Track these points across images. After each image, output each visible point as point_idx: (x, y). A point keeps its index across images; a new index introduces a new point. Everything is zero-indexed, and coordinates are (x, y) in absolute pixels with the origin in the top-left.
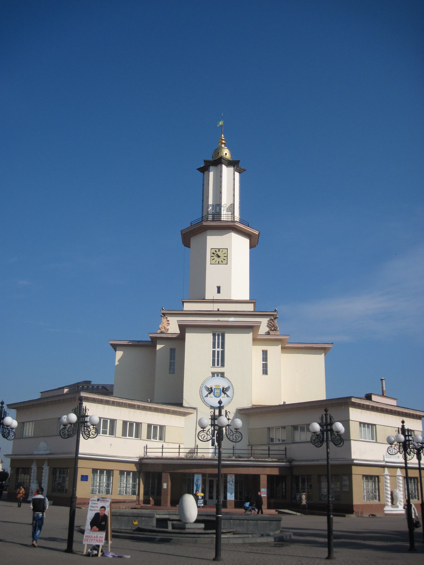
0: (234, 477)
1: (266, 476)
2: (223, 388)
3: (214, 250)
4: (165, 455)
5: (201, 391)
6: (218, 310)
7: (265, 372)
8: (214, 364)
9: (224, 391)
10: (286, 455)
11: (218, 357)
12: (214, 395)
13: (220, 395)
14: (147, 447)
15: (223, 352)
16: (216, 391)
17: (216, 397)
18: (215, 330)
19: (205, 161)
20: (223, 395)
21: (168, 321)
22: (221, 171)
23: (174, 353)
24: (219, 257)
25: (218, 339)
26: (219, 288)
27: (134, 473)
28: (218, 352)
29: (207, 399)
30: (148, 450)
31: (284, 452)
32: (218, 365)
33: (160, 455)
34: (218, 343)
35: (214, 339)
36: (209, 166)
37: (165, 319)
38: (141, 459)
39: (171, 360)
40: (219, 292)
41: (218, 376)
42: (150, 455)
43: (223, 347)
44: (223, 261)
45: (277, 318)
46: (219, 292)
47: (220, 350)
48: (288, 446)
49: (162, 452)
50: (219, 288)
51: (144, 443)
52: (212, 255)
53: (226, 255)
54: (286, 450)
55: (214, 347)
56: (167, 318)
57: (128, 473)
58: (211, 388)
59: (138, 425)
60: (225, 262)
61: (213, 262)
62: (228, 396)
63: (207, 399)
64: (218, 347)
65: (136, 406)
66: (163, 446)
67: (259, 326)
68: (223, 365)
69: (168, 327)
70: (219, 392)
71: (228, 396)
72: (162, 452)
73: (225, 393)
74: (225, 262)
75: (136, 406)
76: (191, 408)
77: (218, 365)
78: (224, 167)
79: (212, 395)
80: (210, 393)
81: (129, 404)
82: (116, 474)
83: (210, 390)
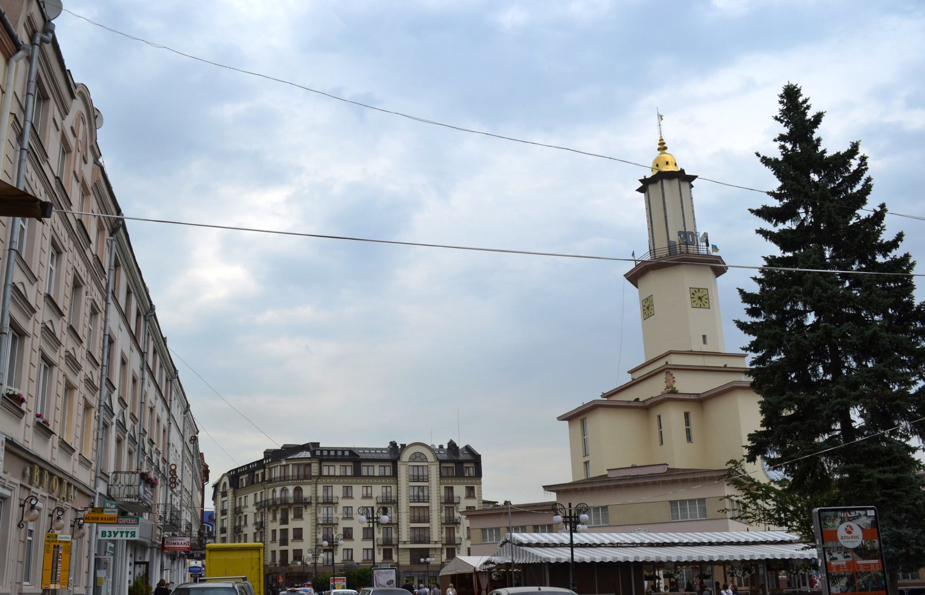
6: (725, 366)
24: (700, 298)
26: (704, 337)
40: (705, 342)
46: (705, 342)
50: (704, 337)
74: (707, 305)
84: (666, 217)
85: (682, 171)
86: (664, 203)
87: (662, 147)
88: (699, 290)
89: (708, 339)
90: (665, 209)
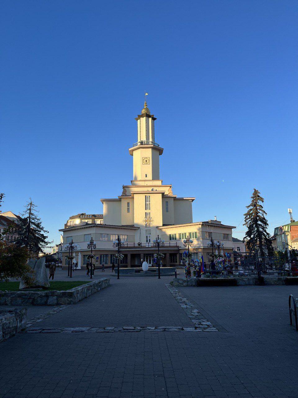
7: (167, 211)
8: (146, 209)
11: (148, 206)
15: (150, 204)
18: (146, 195)
24: (146, 161)
40: (146, 177)
43: (149, 202)
46: (146, 177)
53: (149, 160)
67: (164, 193)
68: (150, 209)
82: (109, 256)
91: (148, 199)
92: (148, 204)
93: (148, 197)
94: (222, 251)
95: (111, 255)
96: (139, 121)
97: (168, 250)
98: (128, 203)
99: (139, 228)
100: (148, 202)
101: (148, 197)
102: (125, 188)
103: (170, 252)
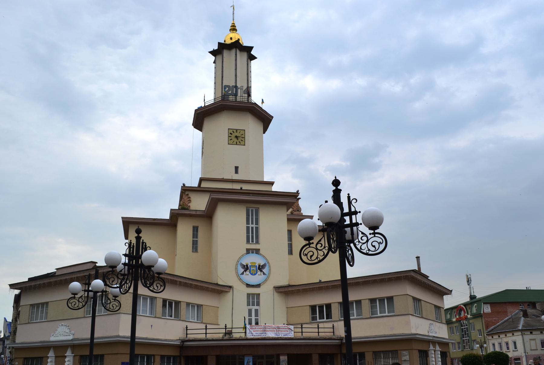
0: (286, 357)
1: (318, 355)
2: (259, 266)
3: (231, 130)
4: (209, 336)
5: (236, 269)
6: (241, 189)
8: (248, 241)
9: (261, 268)
10: (334, 332)
11: (252, 233)
12: (250, 272)
13: (257, 273)
14: (187, 328)
15: (257, 229)
16: (252, 269)
17: (252, 274)
18: (249, 205)
19: (220, 44)
20: (259, 273)
21: (190, 197)
22: (236, 55)
23: (197, 231)
24: (236, 137)
25: (252, 215)
26: (237, 168)
27: (174, 357)
28: (252, 228)
29: (242, 276)
30: (189, 332)
31: (331, 330)
32: (253, 241)
33: (203, 336)
34: (252, 219)
35: (248, 215)
36: (223, 49)
37: (187, 197)
38: (183, 341)
39: (193, 237)
41: (253, 253)
42: (190, 337)
43: (257, 223)
44: (241, 142)
45: (300, 198)
47: (254, 226)
48: (335, 324)
49: (206, 334)
50: (237, 168)
51: (185, 324)
52: (230, 135)
54: (333, 328)
55: (248, 223)
56: (188, 194)
57: (169, 357)
58: (247, 265)
59: (178, 303)
60: (242, 143)
61: (231, 142)
62: (264, 274)
63: (242, 276)
64: (252, 224)
65: (178, 283)
66: (206, 327)
68: (257, 242)
69: (189, 205)
70: (255, 269)
71: (264, 274)
72: (206, 334)
73: (261, 271)
74: (242, 143)
75: (178, 283)
76: (227, 286)
77: (253, 241)
78: (238, 51)
79: (248, 272)
80: (245, 271)
81: (171, 280)
82: (158, 359)
83: (246, 268)
84: (222, 77)
85: (238, 41)
86: (222, 66)
87: (233, 29)
88: (237, 130)
89: (240, 170)
90: (222, 72)
91: (252, 215)
92: (252, 228)
93: (252, 211)
94: (438, 348)
95: (162, 357)
96: (219, 57)
97: (316, 346)
98: (195, 230)
99: (230, 287)
100: (252, 224)
101: (252, 211)
102: (187, 193)
103: (320, 352)
